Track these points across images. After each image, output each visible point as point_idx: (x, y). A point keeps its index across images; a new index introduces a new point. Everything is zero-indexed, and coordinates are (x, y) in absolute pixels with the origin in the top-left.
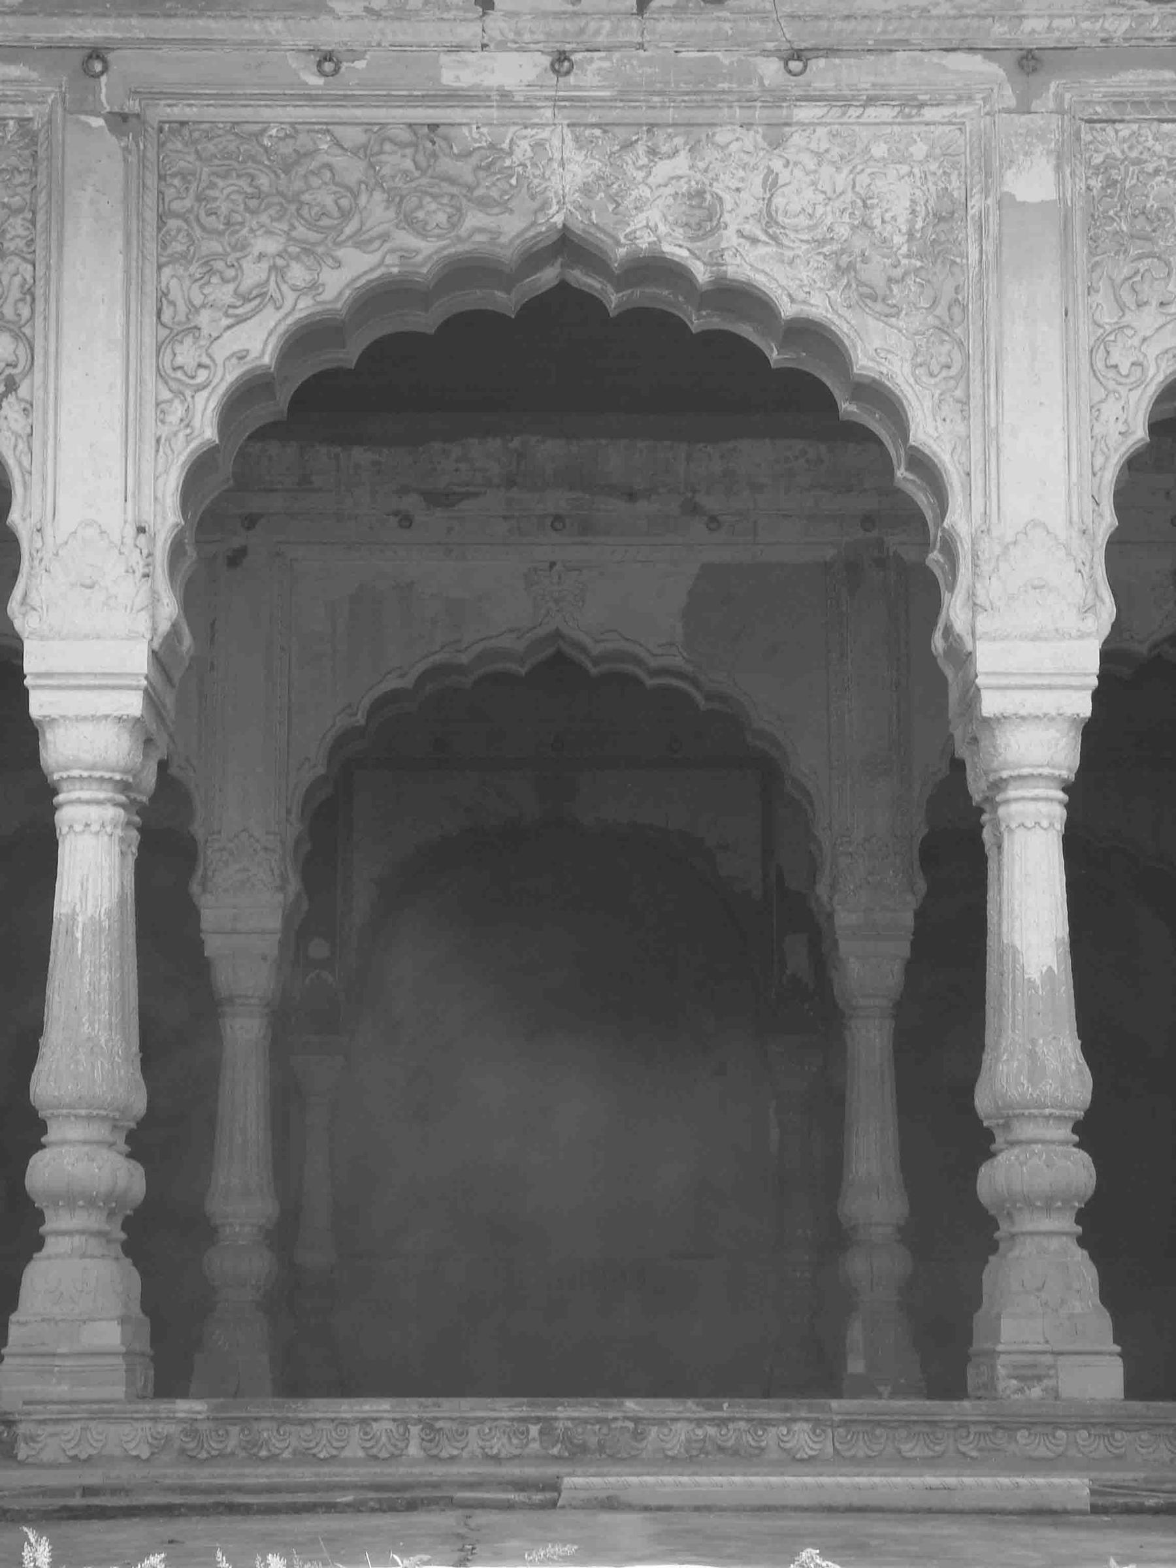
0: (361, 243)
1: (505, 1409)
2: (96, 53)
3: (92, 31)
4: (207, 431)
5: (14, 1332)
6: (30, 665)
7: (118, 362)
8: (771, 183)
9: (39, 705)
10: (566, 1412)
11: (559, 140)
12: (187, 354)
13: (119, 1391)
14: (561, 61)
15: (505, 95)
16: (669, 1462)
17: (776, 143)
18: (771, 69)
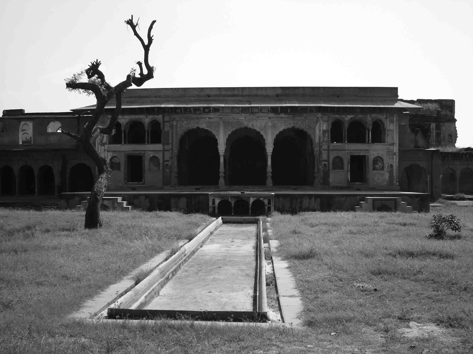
0: (236, 127)
1: (243, 186)
2: (221, 118)
3: (222, 117)
4: (227, 137)
5: (219, 182)
6: (219, 149)
7: (223, 134)
8: (256, 124)
9: (219, 152)
10: (246, 187)
11: (245, 122)
12: (226, 133)
13: (224, 185)
14: (245, 118)
15: (242, 120)
16: (250, 189)
17: (257, 122)
18: (256, 118)
